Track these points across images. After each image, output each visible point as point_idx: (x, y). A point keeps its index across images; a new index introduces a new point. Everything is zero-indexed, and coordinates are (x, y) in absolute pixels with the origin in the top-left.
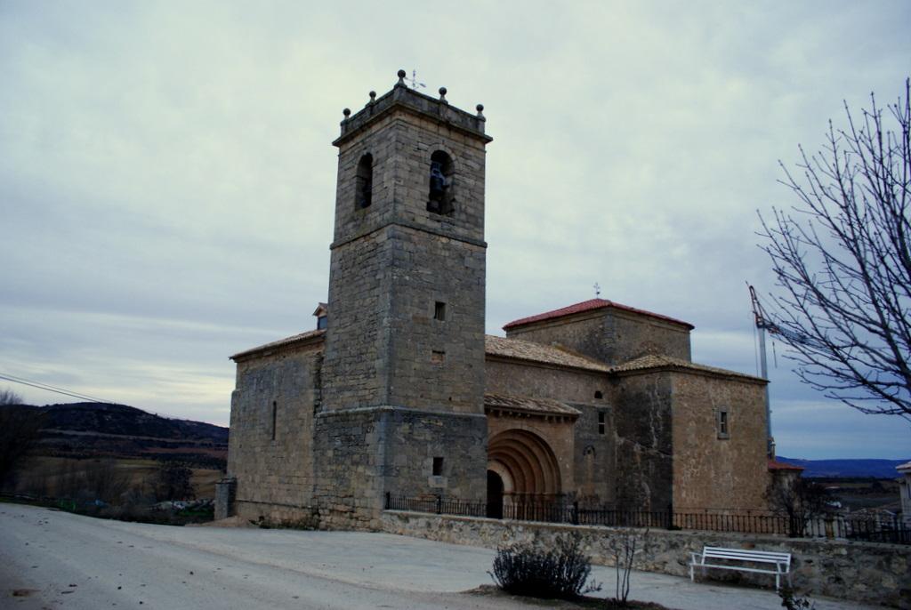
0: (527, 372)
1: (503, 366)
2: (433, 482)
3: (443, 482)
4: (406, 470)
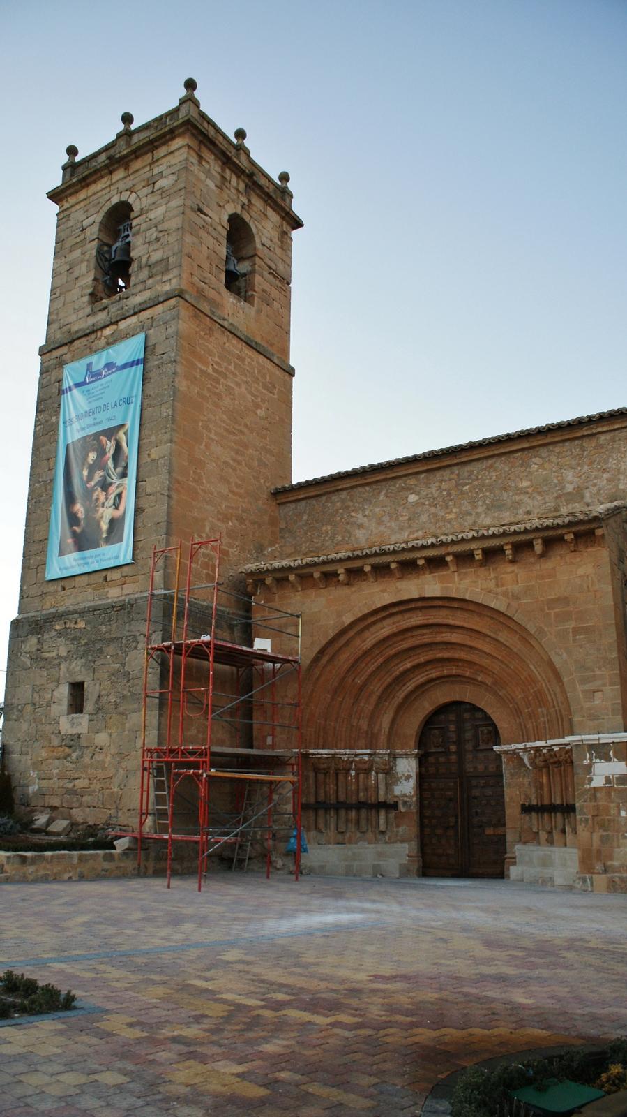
0: (535, 464)
1: (465, 471)
2: (68, 725)
3: (81, 724)
4: (29, 708)
